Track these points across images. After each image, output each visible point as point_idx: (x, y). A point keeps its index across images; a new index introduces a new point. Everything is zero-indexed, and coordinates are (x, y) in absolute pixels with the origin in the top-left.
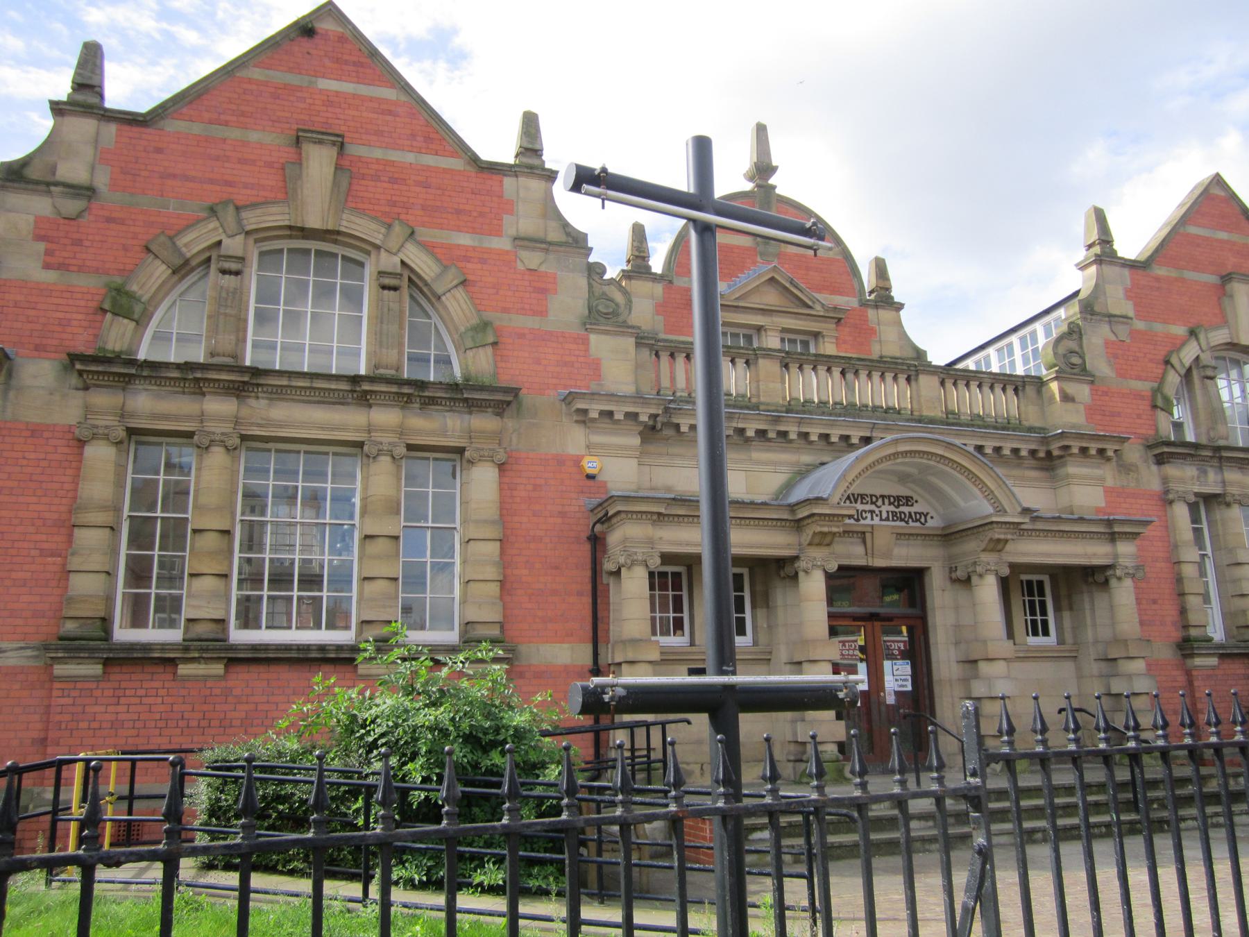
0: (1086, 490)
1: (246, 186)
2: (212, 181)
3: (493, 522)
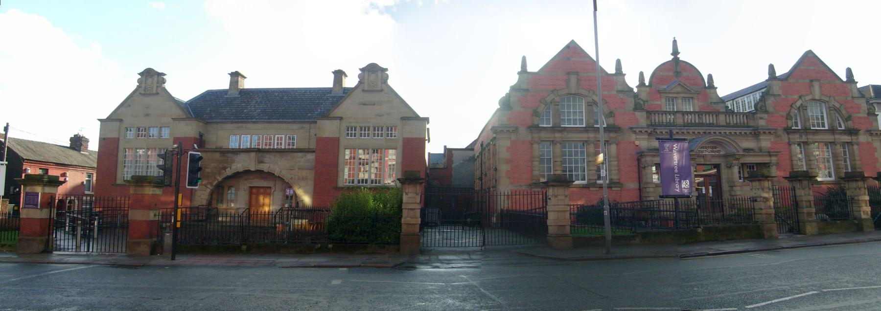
0: (766, 143)
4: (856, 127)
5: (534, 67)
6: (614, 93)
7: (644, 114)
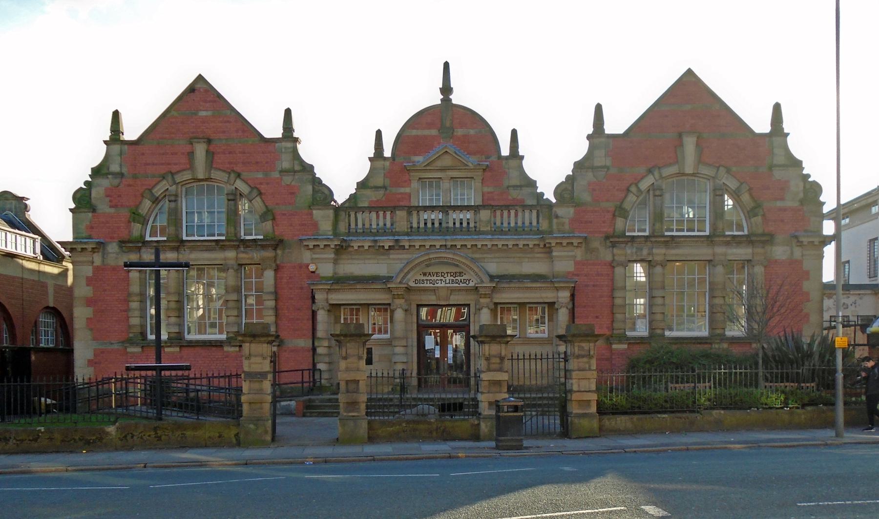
1: (176, 164)
2: (162, 164)
5: (132, 132)
6: (276, 175)
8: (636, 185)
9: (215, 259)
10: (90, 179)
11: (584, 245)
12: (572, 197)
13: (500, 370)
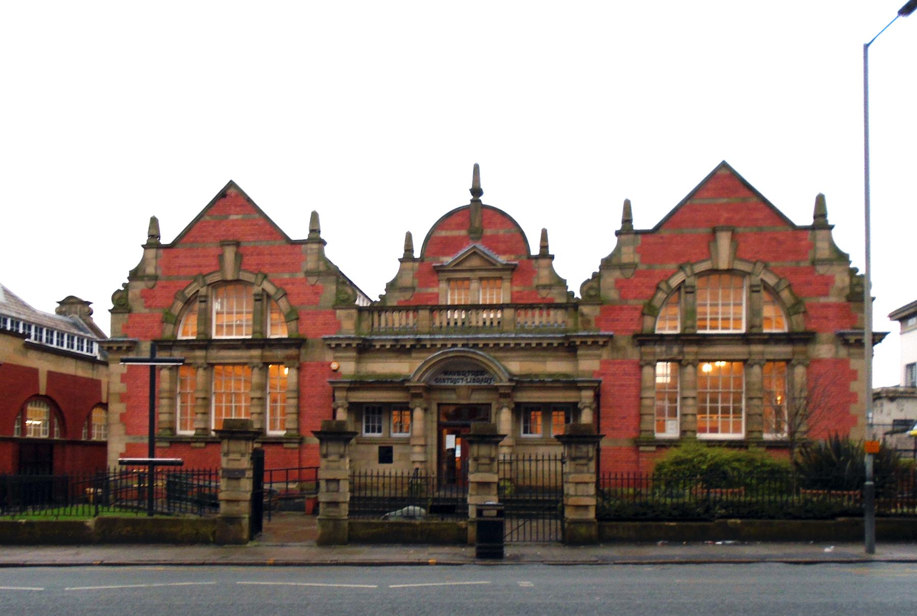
0: (588, 365)
2: (195, 266)
3: (294, 391)
4: (812, 327)
6: (301, 275)
7: (354, 312)
8: (667, 282)
9: (241, 358)
10: (127, 281)
11: (610, 345)
12: (598, 296)
13: (490, 471)
